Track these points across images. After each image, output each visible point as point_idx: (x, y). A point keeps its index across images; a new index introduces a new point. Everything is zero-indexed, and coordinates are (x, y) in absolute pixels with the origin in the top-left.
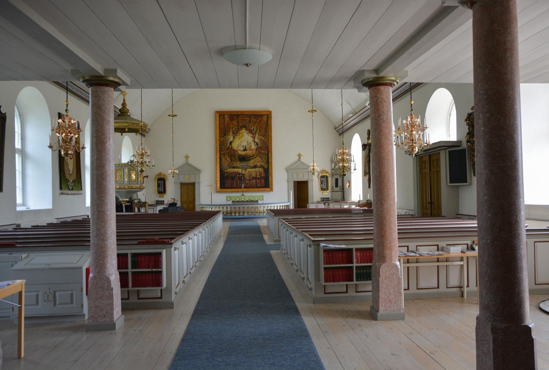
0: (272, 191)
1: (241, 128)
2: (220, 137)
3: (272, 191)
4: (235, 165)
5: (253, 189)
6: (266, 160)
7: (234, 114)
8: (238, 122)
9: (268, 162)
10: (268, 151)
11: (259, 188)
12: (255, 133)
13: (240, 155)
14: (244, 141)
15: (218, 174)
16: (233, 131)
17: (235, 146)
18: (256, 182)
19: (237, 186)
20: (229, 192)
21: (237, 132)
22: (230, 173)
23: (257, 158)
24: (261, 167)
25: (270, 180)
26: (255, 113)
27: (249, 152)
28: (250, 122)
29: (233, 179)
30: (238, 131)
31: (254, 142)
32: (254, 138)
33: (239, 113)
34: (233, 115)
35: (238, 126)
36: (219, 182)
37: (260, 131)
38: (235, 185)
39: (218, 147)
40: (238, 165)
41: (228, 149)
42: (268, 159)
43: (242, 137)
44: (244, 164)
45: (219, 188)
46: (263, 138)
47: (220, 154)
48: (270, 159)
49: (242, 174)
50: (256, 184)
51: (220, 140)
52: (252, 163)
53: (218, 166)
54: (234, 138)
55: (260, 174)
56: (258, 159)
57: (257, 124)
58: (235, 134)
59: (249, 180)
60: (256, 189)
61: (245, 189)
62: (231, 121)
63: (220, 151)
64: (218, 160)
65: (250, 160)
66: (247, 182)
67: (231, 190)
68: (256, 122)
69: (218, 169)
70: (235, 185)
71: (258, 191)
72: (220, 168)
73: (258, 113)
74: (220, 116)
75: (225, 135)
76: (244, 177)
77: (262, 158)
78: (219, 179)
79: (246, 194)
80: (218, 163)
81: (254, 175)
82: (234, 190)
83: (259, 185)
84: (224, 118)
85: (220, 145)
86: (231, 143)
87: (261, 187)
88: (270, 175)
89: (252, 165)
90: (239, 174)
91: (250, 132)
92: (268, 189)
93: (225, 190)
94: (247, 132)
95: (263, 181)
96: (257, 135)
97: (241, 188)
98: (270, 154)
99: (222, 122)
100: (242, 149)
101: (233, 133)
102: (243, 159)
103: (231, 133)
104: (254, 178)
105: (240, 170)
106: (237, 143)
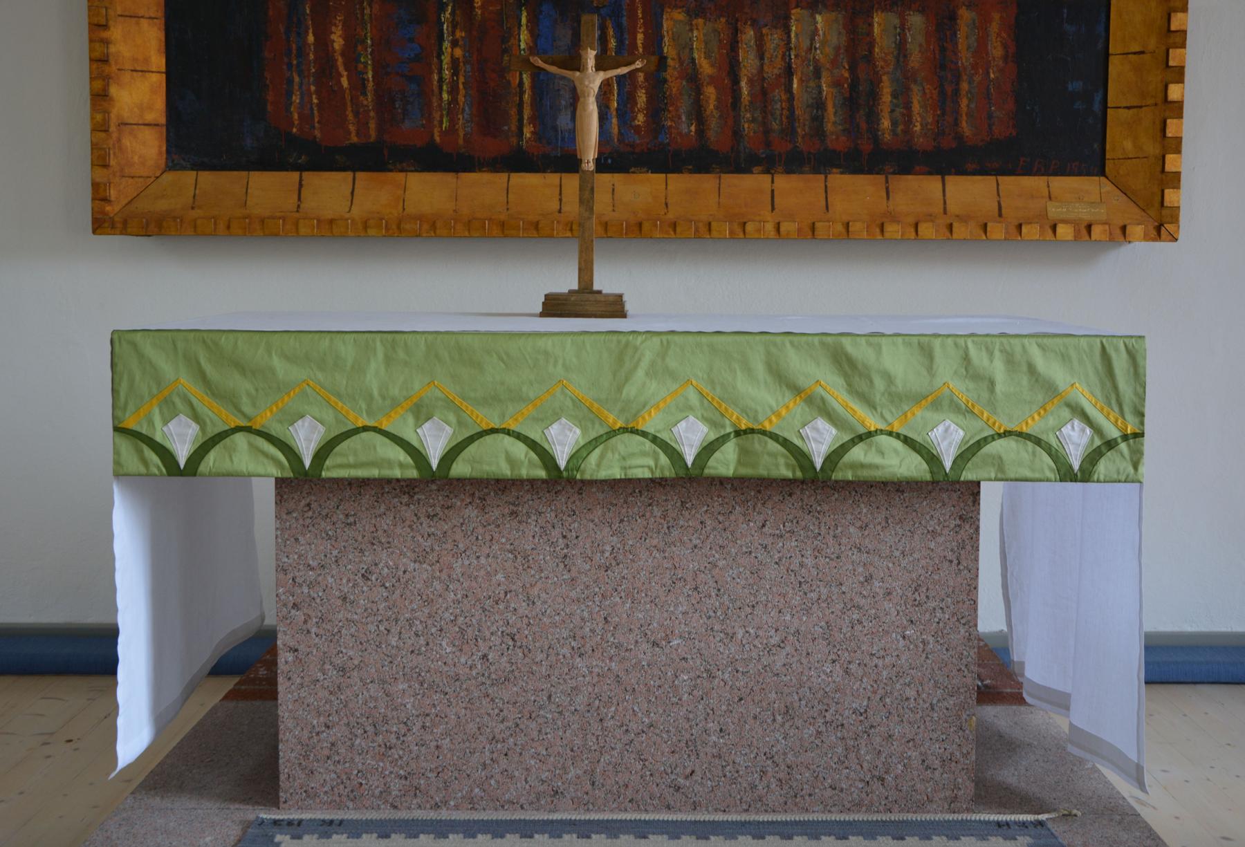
0: (1162, 224)
3: (1162, 224)
5: (795, 190)
18: (857, 48)
20: (332, 232)
38: (449, 111)
45: (147, 147)
50: (859, 99)
60: (856, 192)
61: (640, 190)
67: (375, 193)
71: (876, 233)
79: (666, 292)
82: (426, 190)
83: (904, 113)
87: (948, 159)
92: (1075, 195)
93: (267, 189)
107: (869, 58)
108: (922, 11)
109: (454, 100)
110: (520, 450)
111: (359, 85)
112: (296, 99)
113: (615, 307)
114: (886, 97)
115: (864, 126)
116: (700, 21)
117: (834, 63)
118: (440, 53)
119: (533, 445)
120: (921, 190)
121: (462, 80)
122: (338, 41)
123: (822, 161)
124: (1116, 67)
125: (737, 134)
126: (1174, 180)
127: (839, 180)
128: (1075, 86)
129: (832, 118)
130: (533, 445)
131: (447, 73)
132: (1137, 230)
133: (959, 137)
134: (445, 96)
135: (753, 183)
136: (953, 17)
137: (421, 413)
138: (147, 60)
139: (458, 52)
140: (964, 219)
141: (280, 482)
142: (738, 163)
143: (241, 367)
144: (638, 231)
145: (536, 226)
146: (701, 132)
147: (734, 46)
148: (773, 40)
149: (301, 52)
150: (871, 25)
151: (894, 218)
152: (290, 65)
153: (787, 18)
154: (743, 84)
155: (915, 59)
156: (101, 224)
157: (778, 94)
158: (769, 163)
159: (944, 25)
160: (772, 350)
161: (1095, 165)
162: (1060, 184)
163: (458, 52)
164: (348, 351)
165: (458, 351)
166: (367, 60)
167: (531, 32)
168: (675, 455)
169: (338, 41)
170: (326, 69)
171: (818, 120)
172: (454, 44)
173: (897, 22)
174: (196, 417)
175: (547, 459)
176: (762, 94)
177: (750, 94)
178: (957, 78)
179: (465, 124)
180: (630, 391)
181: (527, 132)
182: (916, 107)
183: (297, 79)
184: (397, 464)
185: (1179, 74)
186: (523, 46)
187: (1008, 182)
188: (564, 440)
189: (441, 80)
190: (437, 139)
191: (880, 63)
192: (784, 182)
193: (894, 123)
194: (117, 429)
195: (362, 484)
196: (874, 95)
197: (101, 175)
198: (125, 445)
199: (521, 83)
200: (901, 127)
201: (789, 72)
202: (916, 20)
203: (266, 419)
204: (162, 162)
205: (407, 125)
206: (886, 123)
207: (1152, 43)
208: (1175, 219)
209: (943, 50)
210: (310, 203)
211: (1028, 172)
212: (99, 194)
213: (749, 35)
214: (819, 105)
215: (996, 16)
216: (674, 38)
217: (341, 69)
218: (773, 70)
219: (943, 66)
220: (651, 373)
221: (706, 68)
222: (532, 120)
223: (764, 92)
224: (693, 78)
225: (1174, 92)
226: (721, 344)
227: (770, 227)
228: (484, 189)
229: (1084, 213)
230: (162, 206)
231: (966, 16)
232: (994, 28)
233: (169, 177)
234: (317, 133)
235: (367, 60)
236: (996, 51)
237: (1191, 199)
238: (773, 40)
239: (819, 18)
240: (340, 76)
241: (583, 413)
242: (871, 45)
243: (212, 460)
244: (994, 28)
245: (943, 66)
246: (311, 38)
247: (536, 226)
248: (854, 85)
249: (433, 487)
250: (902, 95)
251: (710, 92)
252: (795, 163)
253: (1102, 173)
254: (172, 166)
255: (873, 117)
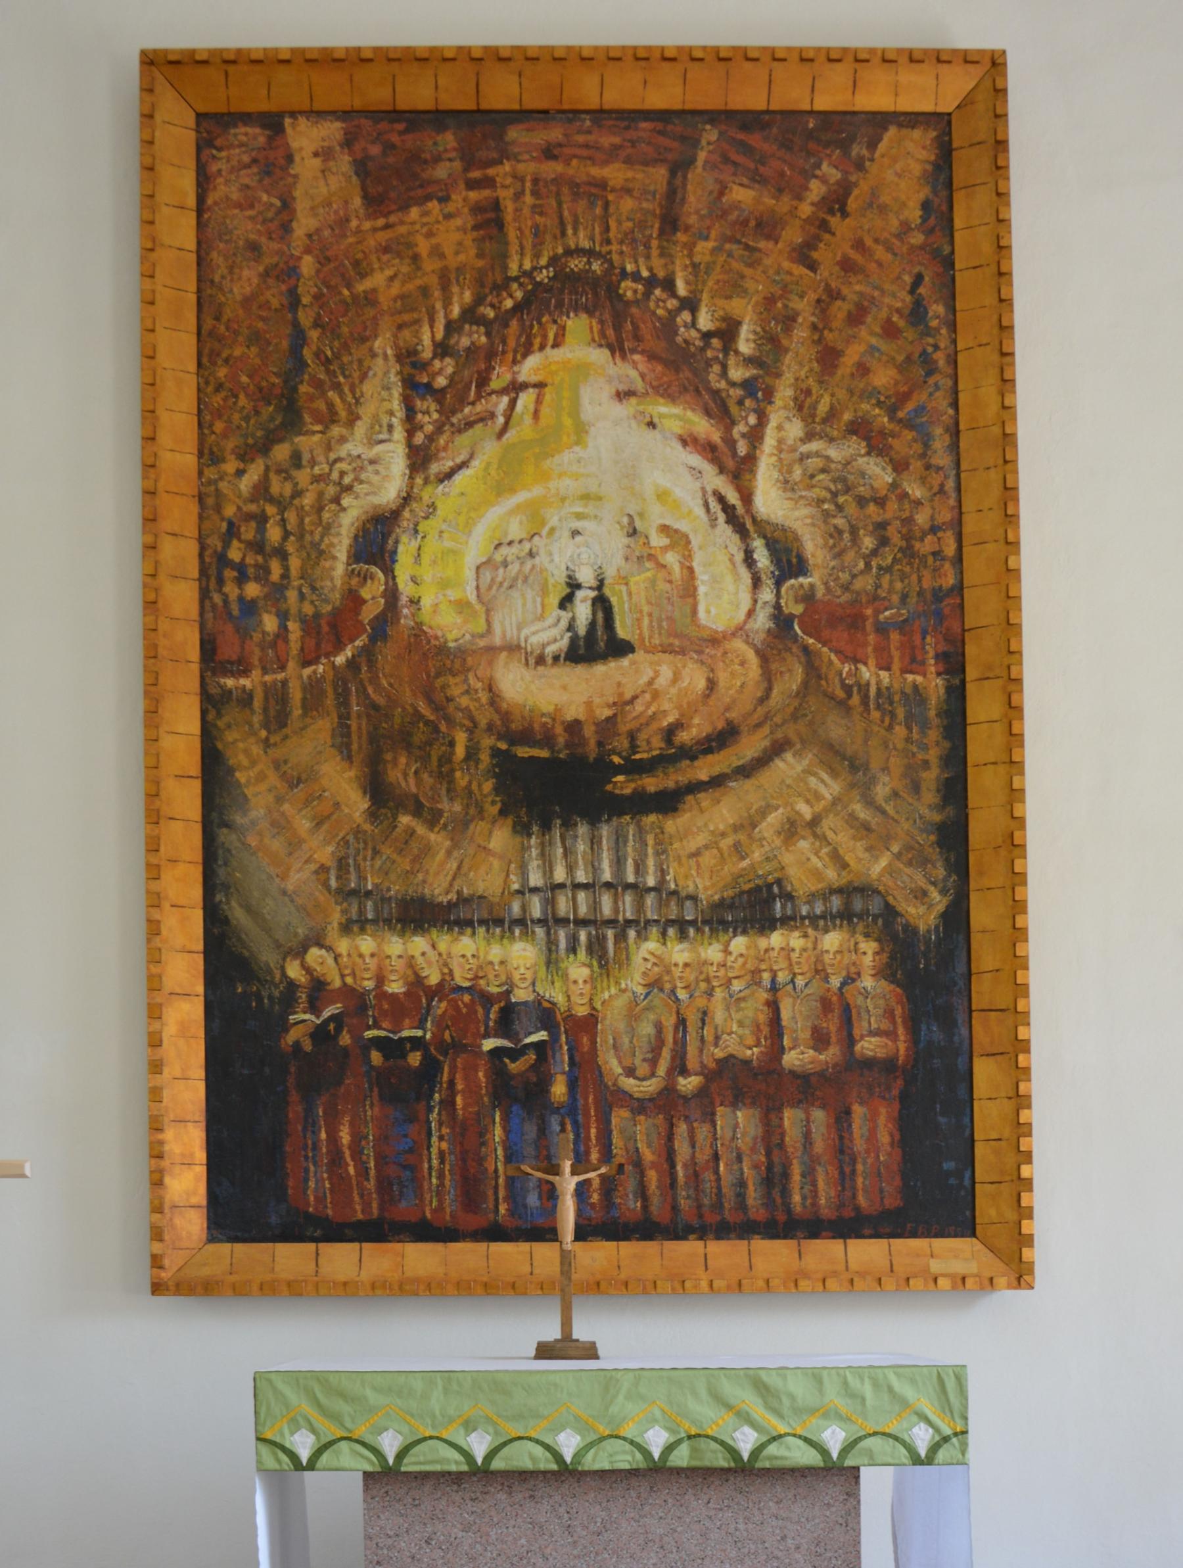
0: (1021, 1275)
1: (543, 305)
2: (208, 455)
4: (438, 886)
5: (724, 1253)
6: (927, 806)
7: (419, 94)
8: (490, 221)
9: (953, 838)
10: (954, 664)
11: (813, 1227)
12: (758, 391)
13: (515, 730)
14: (577, 516)
15: (187, 1013)
16: (408, 358)
17: (440, 580)
18: (772, 1139)
19: (471, 1187)
21: (477, 373)
22: (358, 1003)
23: (787, 766)
24: (853, 904)
25: (987, 1116)
26: (752, 99)
27: (657, 686)
28: (670, 223)
29: (408, 1083)
30: (491, 355)
31: (739, 519)
32: (740, 471)
33: (502, 93)
34: (415, 120)
35: (492, 283)
36: (189, 1142)
37: (829, 358)
38: (438, 1193)
39: (183, 597)
40: (487, 881)
41: (331, 629)
42: (955, 790)
43: (547, 444)
44: (583, 856)
46: (879, 473)
47: (212, 703)
48: (983, 784)
49: (546, 1015)
50: (774, 1178)
51: (207, 500)
52: (698, 847)
53: (185, 886)
54: (419, 459)
55: (840, 1011)
56: (800, 781)
57: (776, 255)
58: (450, 401)
59: (667, 1103)
60: (773, 1254)
61: (598, 1256)
62: (375, 203)
63: (208, 649)
64: (187, 800)
65: (668, 802)
66: (635, 1134)
67: (379, 1259)
68: (767, 227)
69: (186, 930)
70: (438, 1193)
72: (214, 917)
73: (792, 94)
74: (212, 127)
75: (291, 419)
76: (584, 1068)
77: (840, 760)
78: (189, 1092)
80: (185, 839)
81: (735, 1034)
82: (420, 1258)
84: (274, 165)
85: (213, 570)
86: (376, 542)
87: (849, 1226)
88: (984, 1032)
89: (704, 883)
90: (508, 1016)
91: (678, 367)
92: (951, 1254)
93: (290, 1257)
94: (630, 372)
95: (874, 1127)
96: (783, 427)
97: (548, 1233)
98: (982, 706)
99: (243, 226)
100: (550, 634)
101: (415, 387)
102: (565, 782)
103: (382, 392)
104: (739, 1081)
105: (520, 956)
106: (475, 550)
107: (781, 1145)
108: (823, 1107)
109: (441, 1184)
110: (539, 1451)
111: (363, 1172)
112: (312, 1184)
113: (590, 1352)
114: (796, 1177)
115: (779, 1201)
116: (642, 1118)
117: (753, 1149)
118: (429, 1146)
119: (547, 1447)
120: (826, 1252)
121: (447, 1167)
122: (345, 1137)
123: (747, 1229)
124: (980, 1150)
125: (675, 1208)
126: (1029, 1240)
127: (761, 1245)
128: (949, 1165)
129: (753, 1195)
130: (547, 1447)
131: (435, 1162)
132: (1002, 1281)
133: (857, 1208)
134: (434, 1181)
135: (691, 1247)
136: (848, 1112)
137: (469, 1426)
138: (192, 1155)
139: (444, 1145)
140: (862, 1275)
141: (367, 1475)
142: (676, 1231)
143: (342, 1395)
144: (596, 1287)
145: (513, 1286)
146: (645, 1207)
147: (670, 1137)
148: (703, 1131)
149: (315, 1147)
150: (781, 1119)
151: (806, 1275)
152: (306, 1157)
153: (713, 1114)
154: (679, 1168)
155: (819, 1146)
156: (157, 1288)
157: (708, 1176)
158: (702, 1232)
159: (842, 1118)
160: (711, 1381)
161: (967, 1228)
162: (939, 1244)
163: (444, 1145)
164: (418, 1385)
165: (493, 1385)
166: (369, 1152)
167: (504, 1128)
168: (646, 1453)
169: (345, 1137)
170: (336, 1159)
171: (741, 1196)
172: (441, 1138)
173: (803, 1116)
174: (313, 1431)
175: (558, 1457)
176: (695, 1176)
177: (686, 1176)
178: (854, 1161)
179: (451, 1203)
180: (614, 1409)
181: (503, 1209)
182: (821, 1184)
183: (312, 1168)
184: (454, 1462)
185: (1028, 1157)
186: (497, 1139)
187: (897, 1243)
188: (569, 1444)
189: (430, 1168)
190: (428, 1215)
191: (790, 1150)
192: (716, 1248)
193: (804, 1198)
194: (258, 1439)
195: (425, 1476)
196: (786, 1175)
197: (157, 1248)
198: (265, 1450)
199: (496, 1170)
200: (809, 1201)
201: (716, 1157)
202: (819, 1115)
203: (361, 1431)
204: (204, 1236)
205: (403, 1204)
206: (797, 1198)
207: (1007, 1132)
208: (1031, 1271)
209: (841, 1138)
210: (326, 1269)
211: (914, 1235)
212: (156, 1261)
213: (682, 1128)
214: (742, 1184)
215: (883, 1111)
216: (622, 1132)
217: (349, 1159)
218: (703, 1156)
219: (842, 1151)
220: (628, 1397)
221: (648, 1156)
222: (506, 1199)
223: (696, 1175)
224: (638, 1164)
225: (1025, 1171)
226: (676, 1379)
227: (704, 1284)
228: (468, 1256)
229: (959, 1267)
230: (206, 1272)
231: (858, 1111)
232: (882, 1120)
233: (211, 1247)
234: (330, 1212)
235: (369, 1152)
236: (884, 1138)
237: (1041, 1255)
238: (703, 1131)
239: (739, 1114)
240: (347, 1165)
241: (581, 1426)
242: (783, 1135)
243: (325, 1459)
244: (882, 1120)
245: (842, 1151)
246: (323, 1135)
247: (513, 1286)
248: (770, 1168)
249: (480, 1477)
250: (809, 1174)
251: (652, 1176)
252: (723, 1231)
253: (974, 1235)
254: (211, 1239)
255: (785, 1193)
